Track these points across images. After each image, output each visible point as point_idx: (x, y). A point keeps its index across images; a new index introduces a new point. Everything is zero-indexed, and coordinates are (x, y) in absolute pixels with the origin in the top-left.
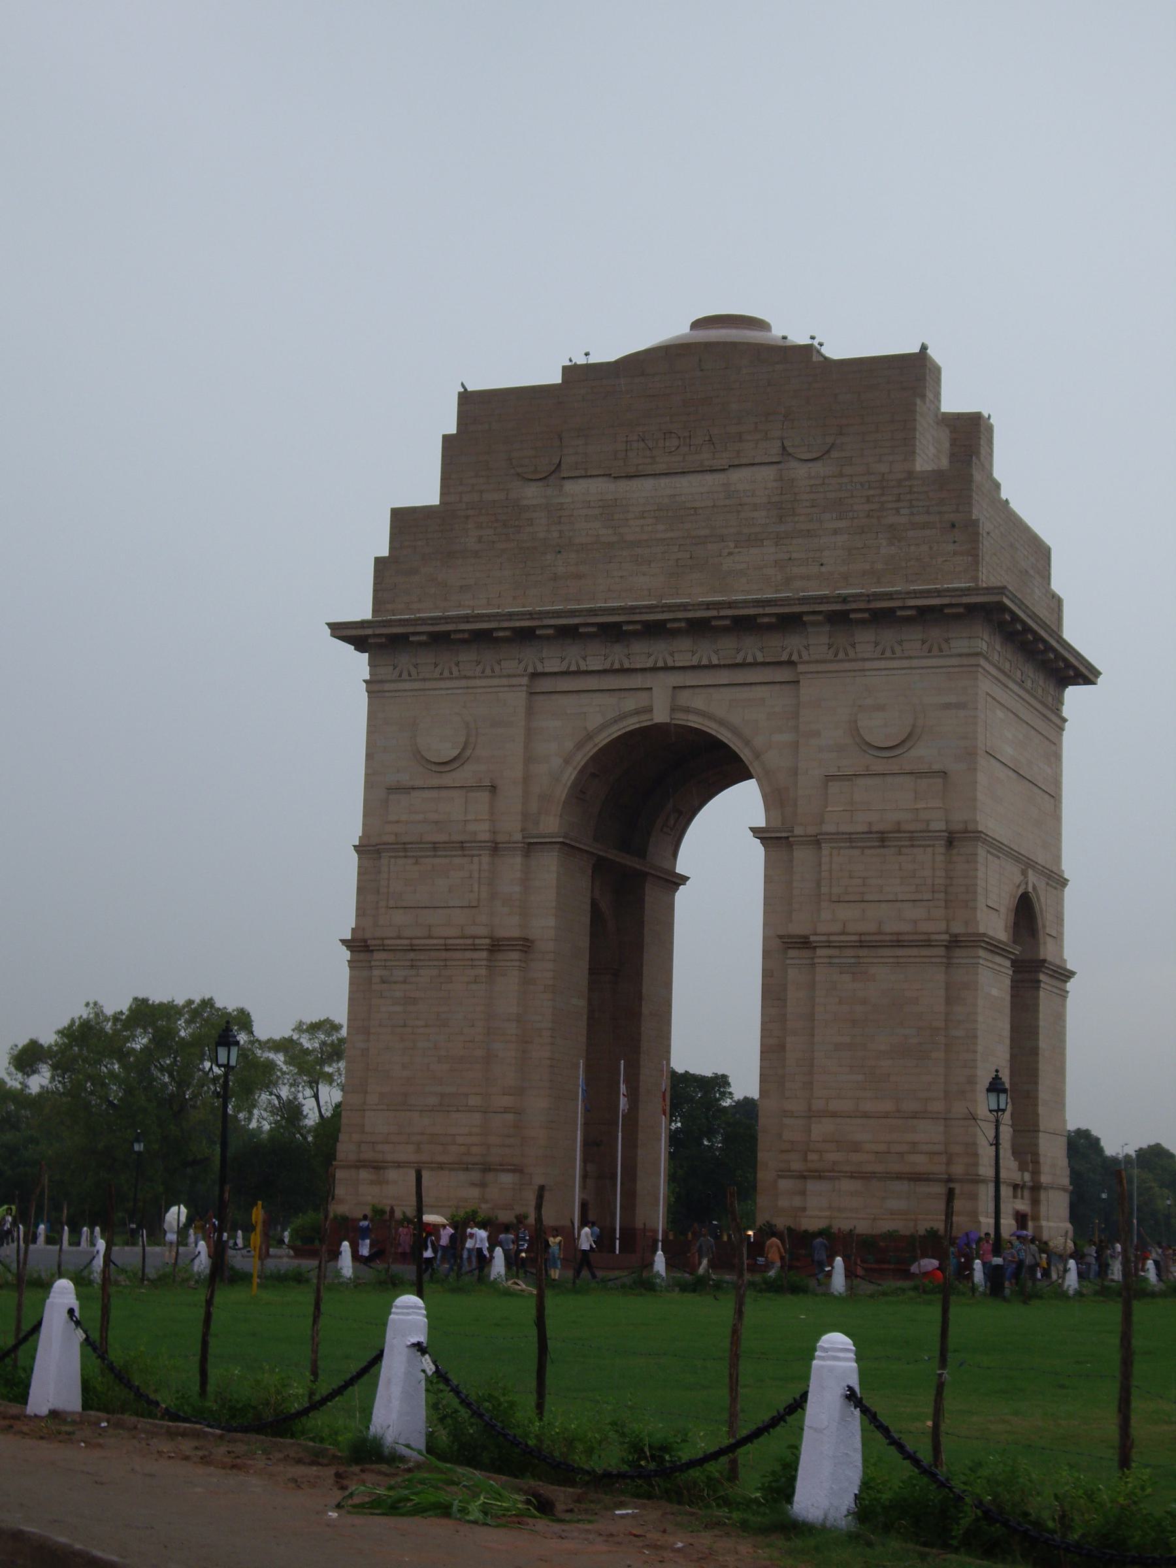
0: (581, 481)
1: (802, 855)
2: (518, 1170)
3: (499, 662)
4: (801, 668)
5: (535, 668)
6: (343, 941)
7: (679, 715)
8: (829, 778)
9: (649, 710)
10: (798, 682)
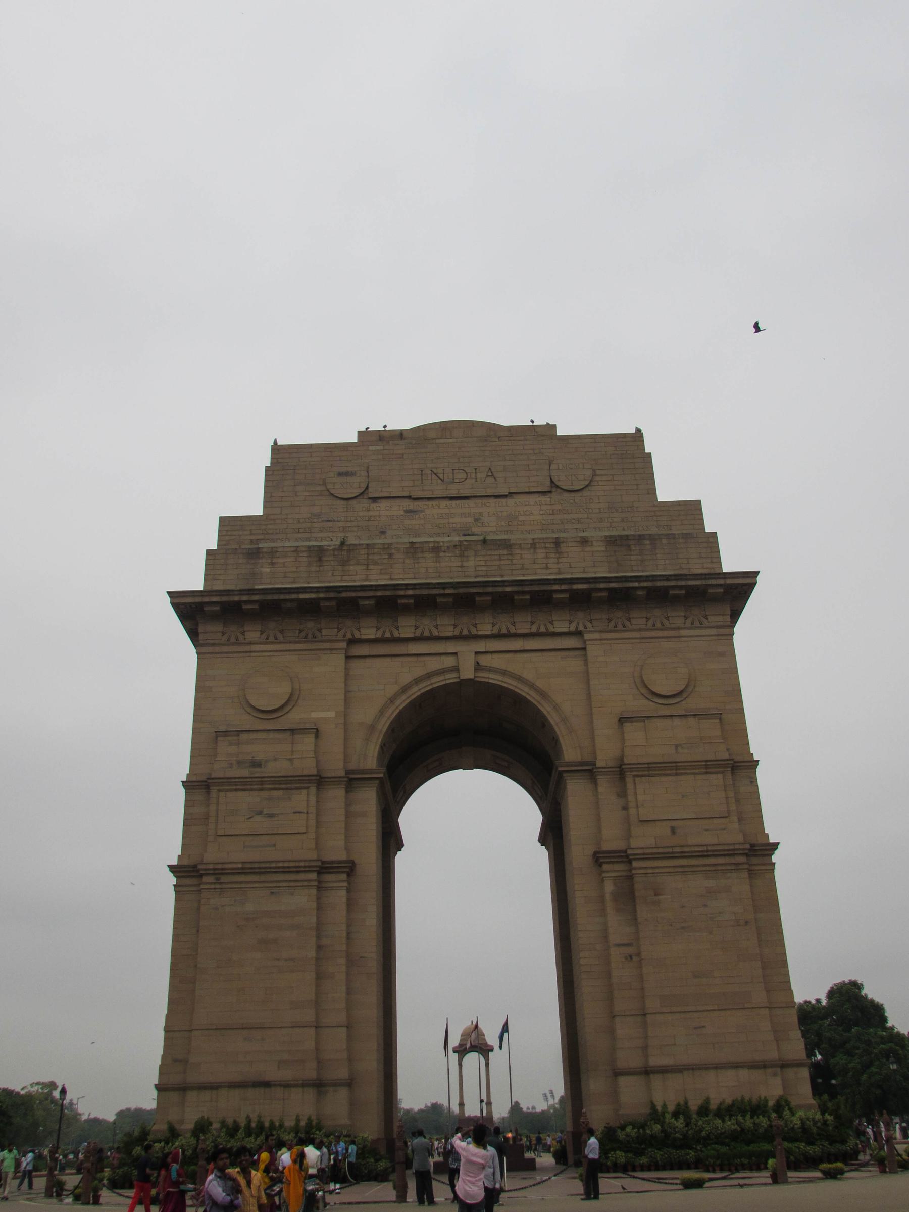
0: (384, 501)
1: (605, 785)
2: (350, 1084)
3: (320, 630)
4: (587, 636)
5: (353, 635)
6: (171, 867)
7: (481, 674)
8: (622, 720)
9: (456, 669)
10: (584, 649)
